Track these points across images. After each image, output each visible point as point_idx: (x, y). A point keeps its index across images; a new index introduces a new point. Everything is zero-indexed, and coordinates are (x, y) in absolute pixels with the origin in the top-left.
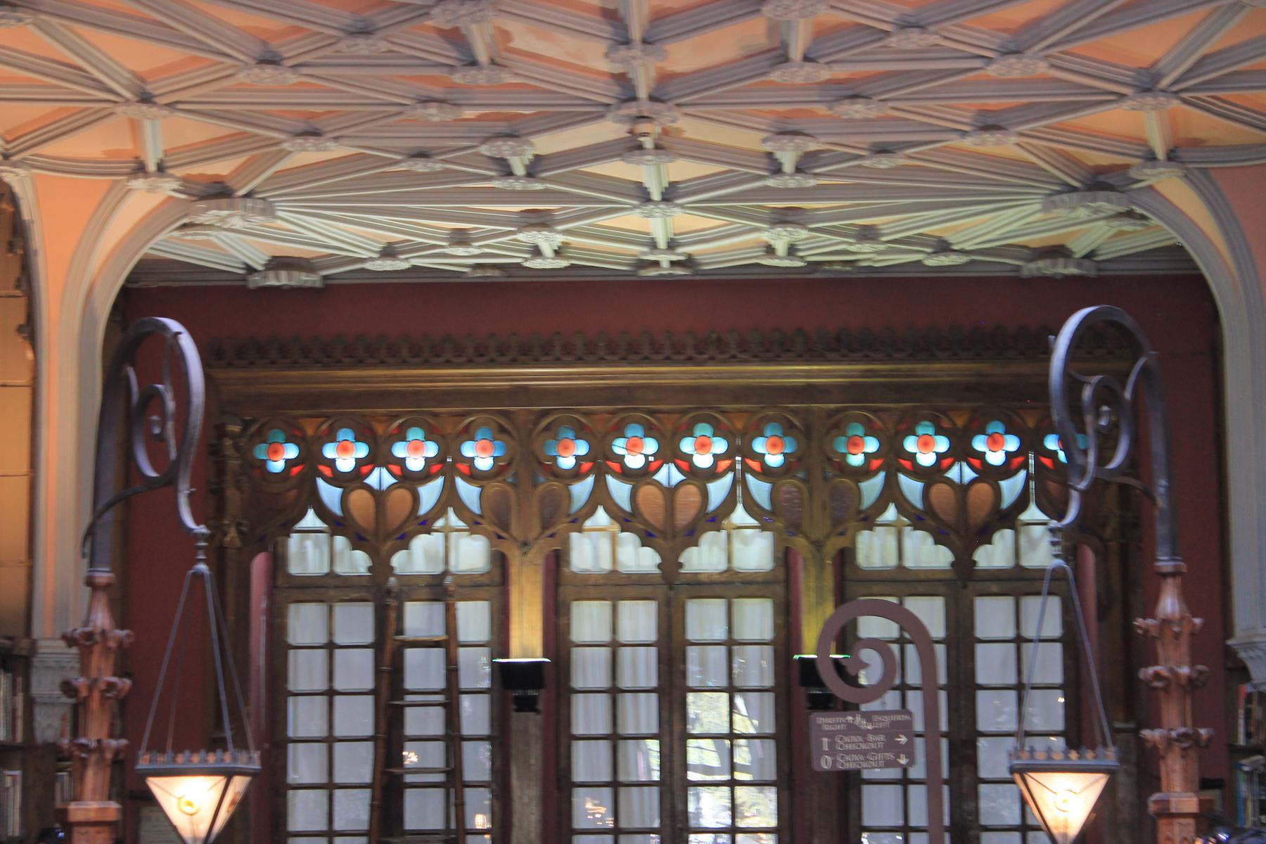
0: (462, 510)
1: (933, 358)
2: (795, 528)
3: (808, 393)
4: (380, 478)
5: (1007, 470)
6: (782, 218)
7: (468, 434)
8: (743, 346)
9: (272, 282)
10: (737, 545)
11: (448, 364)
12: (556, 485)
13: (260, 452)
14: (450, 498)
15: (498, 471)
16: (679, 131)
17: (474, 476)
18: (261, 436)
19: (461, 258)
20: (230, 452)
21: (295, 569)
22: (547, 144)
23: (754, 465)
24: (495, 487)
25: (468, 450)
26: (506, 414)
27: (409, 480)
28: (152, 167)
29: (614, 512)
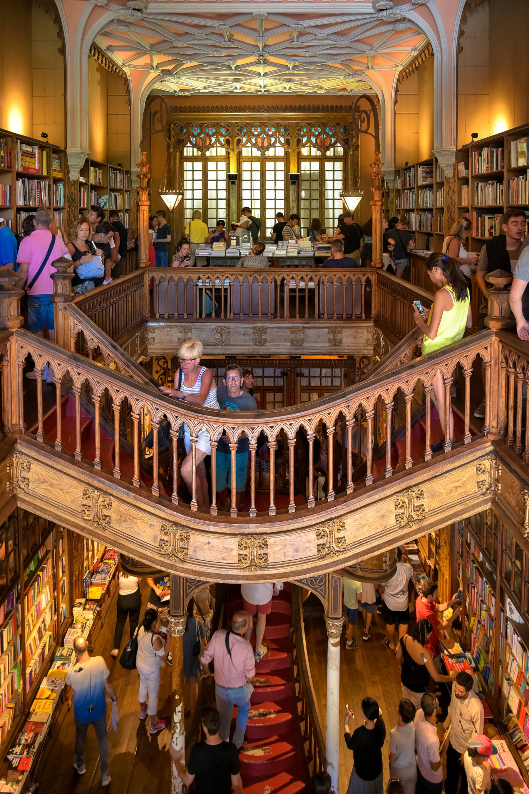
6: (288, 81)
16: (268, 60)
19: (220, 90)
22: (240, 62)
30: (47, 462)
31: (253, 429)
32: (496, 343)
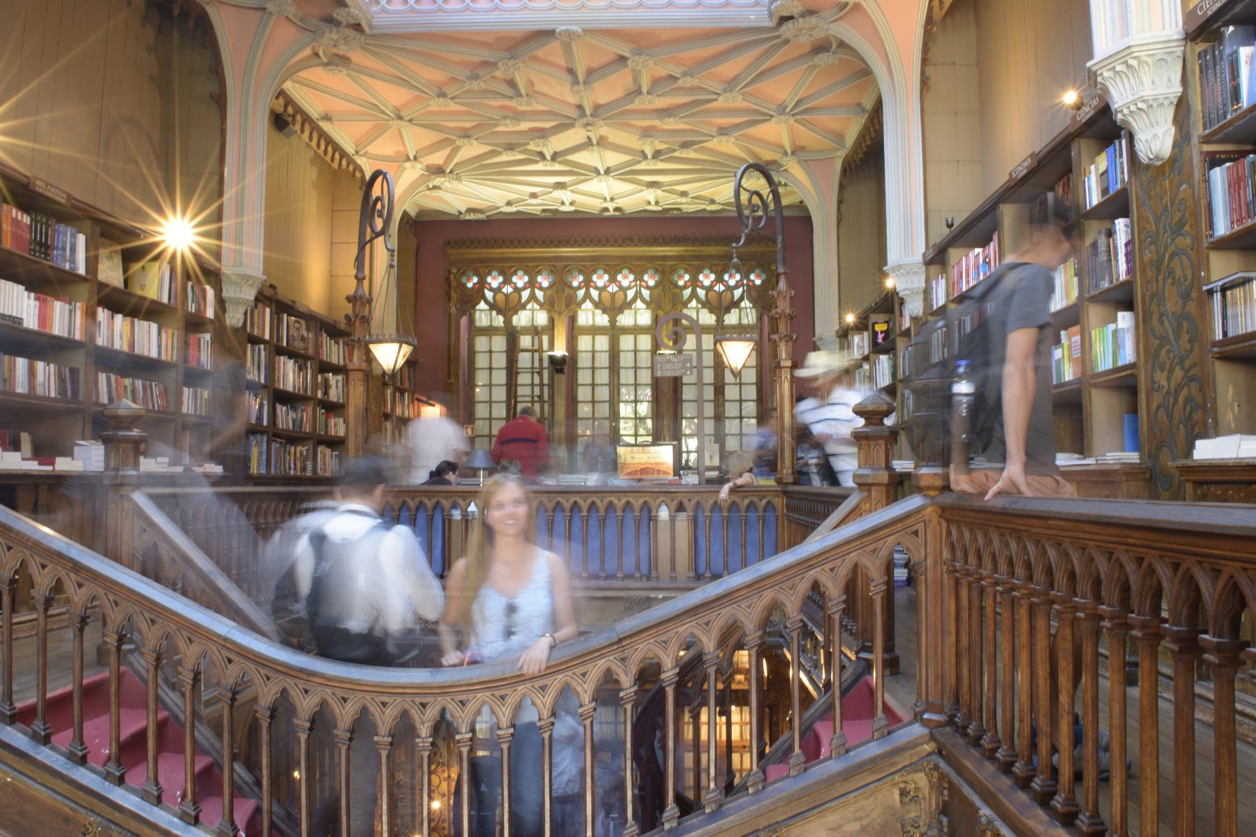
0: (537, 301)
1: (709, 245)
2: (659, 307)
3: (664, 258)
4: (508, 289)
5: (736, 287)
7: (539, 273)
8: (640, 240)
9: (468, 217)
10: (638, 316)
11: (532, 247)
12: (571, 291)
13: (464, 280)
14: (533, 297)
15: (550, 287)
17: (541, 288)
18: (464, 273)
20: (453, 279)
21: (478, 324)
23: (643, 284)
24: (549, 292)
25: (539, 279)
26: (554, 266)
27: (518, 291)
28: (412, 158)
29: (592, 301)
30: (15, 765)
31: (424, 705)
32: (935, 519)
